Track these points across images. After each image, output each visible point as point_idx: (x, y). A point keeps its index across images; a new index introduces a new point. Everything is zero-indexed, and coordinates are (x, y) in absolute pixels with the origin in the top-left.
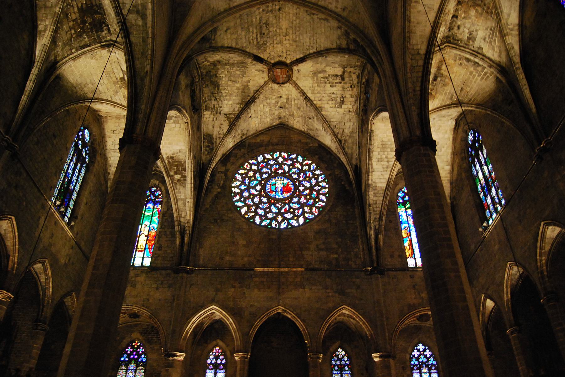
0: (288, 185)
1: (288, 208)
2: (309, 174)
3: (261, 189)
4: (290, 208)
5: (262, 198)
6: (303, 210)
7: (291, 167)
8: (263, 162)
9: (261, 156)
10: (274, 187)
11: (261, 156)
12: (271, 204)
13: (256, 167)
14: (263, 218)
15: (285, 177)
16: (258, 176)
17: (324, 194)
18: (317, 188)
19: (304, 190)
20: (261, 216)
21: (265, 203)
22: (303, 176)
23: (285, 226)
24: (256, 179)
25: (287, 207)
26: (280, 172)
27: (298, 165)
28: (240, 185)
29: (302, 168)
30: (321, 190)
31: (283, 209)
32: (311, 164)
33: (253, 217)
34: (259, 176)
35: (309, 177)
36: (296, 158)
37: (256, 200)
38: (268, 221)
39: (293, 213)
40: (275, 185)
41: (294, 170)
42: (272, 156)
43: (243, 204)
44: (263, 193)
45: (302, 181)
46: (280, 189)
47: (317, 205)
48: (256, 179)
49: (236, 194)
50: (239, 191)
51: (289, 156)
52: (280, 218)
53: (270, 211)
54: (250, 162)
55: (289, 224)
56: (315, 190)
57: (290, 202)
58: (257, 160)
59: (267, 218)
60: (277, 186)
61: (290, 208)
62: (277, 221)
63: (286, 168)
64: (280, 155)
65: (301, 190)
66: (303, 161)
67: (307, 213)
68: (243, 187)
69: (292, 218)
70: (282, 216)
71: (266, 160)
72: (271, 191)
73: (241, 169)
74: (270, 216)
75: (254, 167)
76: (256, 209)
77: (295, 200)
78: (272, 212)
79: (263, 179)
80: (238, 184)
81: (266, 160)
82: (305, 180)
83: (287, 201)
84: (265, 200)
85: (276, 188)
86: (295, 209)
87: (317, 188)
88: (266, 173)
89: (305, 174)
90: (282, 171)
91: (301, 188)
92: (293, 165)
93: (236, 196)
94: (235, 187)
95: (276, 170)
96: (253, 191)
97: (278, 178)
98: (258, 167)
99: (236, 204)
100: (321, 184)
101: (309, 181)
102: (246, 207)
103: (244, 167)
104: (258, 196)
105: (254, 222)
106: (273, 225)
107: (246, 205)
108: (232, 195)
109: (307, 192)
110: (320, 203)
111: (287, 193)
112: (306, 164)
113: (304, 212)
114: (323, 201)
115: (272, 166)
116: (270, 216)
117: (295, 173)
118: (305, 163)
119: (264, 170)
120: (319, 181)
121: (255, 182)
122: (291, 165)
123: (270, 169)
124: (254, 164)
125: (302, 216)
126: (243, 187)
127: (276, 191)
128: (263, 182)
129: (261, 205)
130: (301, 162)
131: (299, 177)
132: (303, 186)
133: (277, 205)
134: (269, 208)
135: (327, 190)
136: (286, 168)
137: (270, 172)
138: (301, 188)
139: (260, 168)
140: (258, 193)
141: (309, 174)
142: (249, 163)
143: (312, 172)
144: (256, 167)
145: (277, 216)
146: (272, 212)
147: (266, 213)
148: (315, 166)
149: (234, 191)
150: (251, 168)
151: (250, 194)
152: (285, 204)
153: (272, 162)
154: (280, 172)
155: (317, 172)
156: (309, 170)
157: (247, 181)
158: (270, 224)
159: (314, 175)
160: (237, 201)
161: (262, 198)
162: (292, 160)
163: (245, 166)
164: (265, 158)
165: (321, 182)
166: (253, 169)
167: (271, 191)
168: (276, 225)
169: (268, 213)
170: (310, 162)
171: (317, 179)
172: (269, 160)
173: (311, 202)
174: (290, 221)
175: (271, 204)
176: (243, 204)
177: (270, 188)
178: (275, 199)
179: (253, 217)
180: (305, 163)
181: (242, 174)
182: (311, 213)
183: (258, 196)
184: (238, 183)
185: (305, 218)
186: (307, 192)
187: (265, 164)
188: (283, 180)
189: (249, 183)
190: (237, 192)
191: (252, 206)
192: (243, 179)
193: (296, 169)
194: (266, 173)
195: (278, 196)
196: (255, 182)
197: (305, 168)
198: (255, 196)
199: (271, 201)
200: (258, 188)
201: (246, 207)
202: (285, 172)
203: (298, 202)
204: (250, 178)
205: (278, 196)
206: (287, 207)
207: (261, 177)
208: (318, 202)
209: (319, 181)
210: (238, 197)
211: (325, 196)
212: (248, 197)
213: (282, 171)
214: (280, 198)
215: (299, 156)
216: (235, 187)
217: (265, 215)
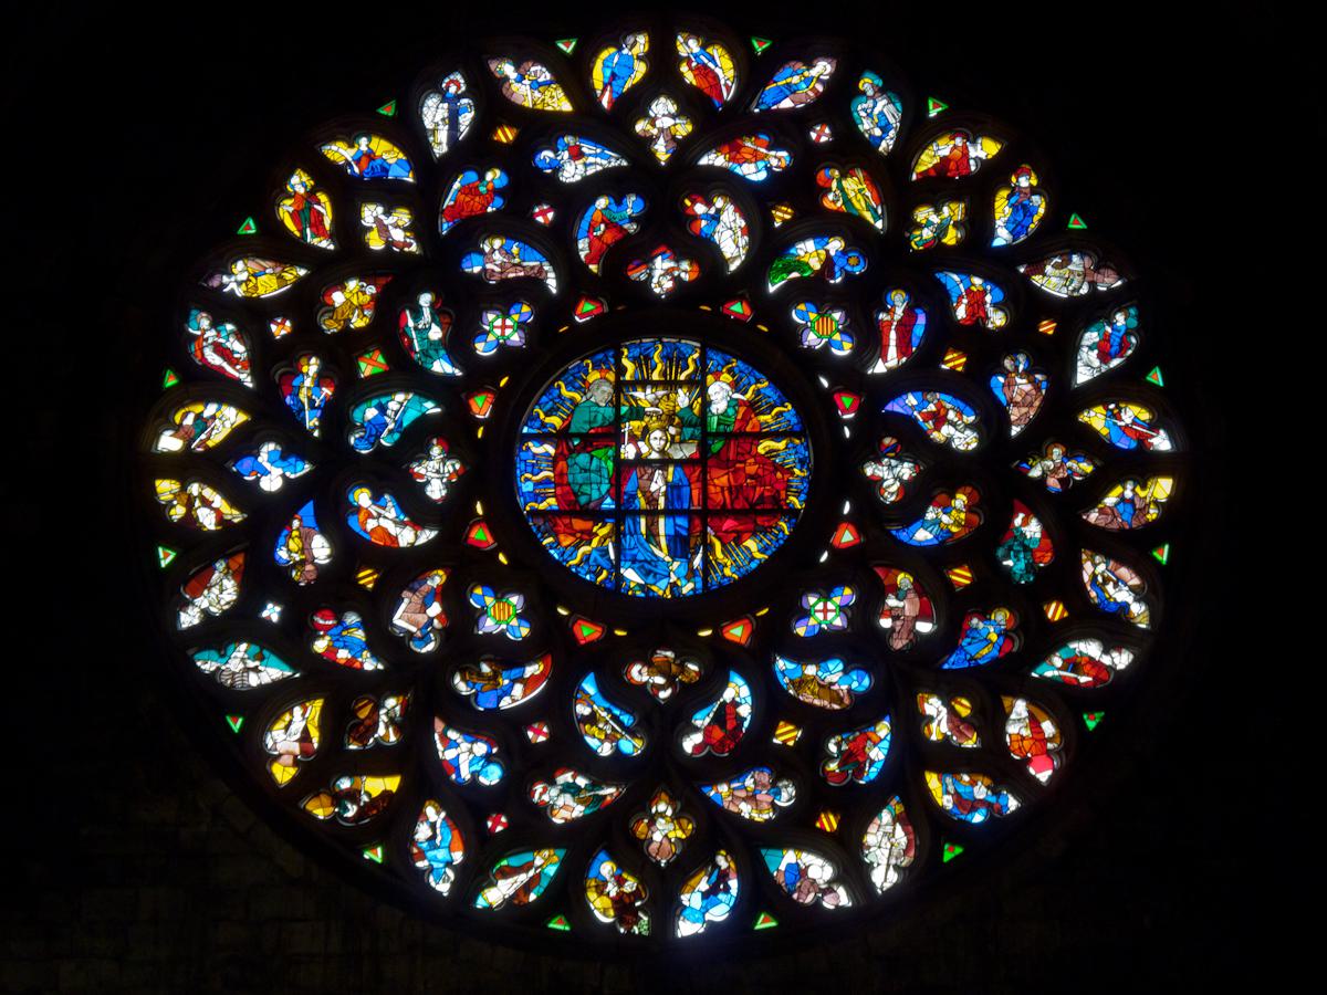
0: (741, 437)
1: (745, 711)
2: (976, 302)
3: (461, 491)
4: (773, 702)
5: (481, 597)
6: (910, 725)
7: (782, 215)
8: (473, 152)
9: (456, 83)
10: (603, 460)
11: (456, 83)
12: (568, 664)
13: (403, 216)
14: (498, 825)
15: (724, 340)
16: (425, 327)
17: (1126, 546)
18: (1052, 467)
19: (913, 502)
20: (467, 805)
21: (508, 655)
22: (905, 327)
23: (719, 913)
24: (407, 373)
25: (738, 691)
26: (663, 274)
27: (853, 192)
28: (242, 443)
29: (902, 221)
30: (1091, 490)
31: (702, 719)
32: (994, 175)
33: (393, 819)
34: (436, 333)
35: (973, 337)
36: (836, 102)
37: (414, 616)
38: (547, 863)
39: (800, 765)
40: (610, 435)
41: (809, 252)
42: (573, 76)
43: (273, 672)
44: (480, 534)
45: (897, 383)
46: (658, 485)
47: (1053, 668)
48: (407, 373)
49: (200, 551)
50: (235, 515)
51: (755, 74)
52: (664, 831)
53: (568, 751)
54: (339, 152)
55: (761, 891)
56: (1035, 498)
57: (776, 638)
58: (410, 135)
59: (533, 829)
60: (629, 452)
61: (773, 702)
62: (632, 855)
63: (730, 237)
64: (663, 65)
65: (891, 492)
66: (916, 133)
67: (949, 759)
68: (272, 474)
69: (793, 829)
70: (693, 805)
71: (505, 135)
72: (576, 510)
73: (249, 249)
74: (563, 802)
75: (387, 227)
76: (414, 728)
77: (825, 613)
78: (585, 761)
79: (479, 374)
80: (218, 435)
81: (505, 135)
82: (920, 373)
83: (737, 632)
84: (502, 616)
85: (623, 468)
86: (818, 724)
87: (1052, 467)
88: (507, 294)
89: (933, 299)
90: (686, 271)
91: (892, 475)
92: (799, 186)
93: (203, 585)
94: (186, 466)
95: (626, 251)
96: (380, 518)
97: (643, 361)
98: (422, 227)
99: (207, 664)
100: (1096, 418)
101: (974, 390)
102: (316, 707)
103: (271, 226)
104: (437, 579)
105: (403, 871)
106: (601, 908)
107: (318, 678)
108: (166, 557)
109: (947, 518)
110: (1092, 649)
111: (734, 540)
112: (940, 187)
113: (914, 755)
114: (1112, 629)
115: (574, 200)
116: (563, 802)
117: (814, 289)
118: (927, 160)
119: (495, 258)
120: (1083, 376)
121: (403, 407)
122: (778, 187)
123: (557, 243)
124: (388, 193)
125: (896, 805)
126: (272, 474)
127: (623, 514)
128: (481, 406)
129: (470, 672)
130: (886, 145)
131: (869, 340)
132: (912, 441)
133: (638, 673)
134: (556, 704)
135: (1162, 488)
136: (730, 237)
137: (552, 283)
138: (892, 475)
139: (445, 227)
140: (427, 535)
141: (976, 302)
142: (330, 178)
143: (1008, 269)
144: (403, 216)
145: (636, 805)
146: (585, 761)
147: (525, 766)
148: (1040, 204)
149: (178, 512)
150: (349, 229)
151: (352, 549)
152: (722, 661)
153: (577, 164)
154: (663, 274)
155: (1057, 280)
156: (975, 252)
157: (309, 385)
158: (568, 892)
159: (1025, 303)
160: (218, 632)
161: (481, 597)
162: (787, 129)
163: (285, 211)
164: (492, 102)
165: (1108, 390)
166: (376, 243)
167: (576, 510)
168: (623, 906)
169: (543, 765)
170: (986, 149)
171: (1055, 359)
172: (541, 127)
173: (989, 634)
174: (769, 856)
175: (568, 664)
176: (273, 672)
177: (560, 480)
178: (607, 601)
179: (393, 819)
180: (927, 160)
181: (250, 315)
182: (998, 764)
183: (437, 579)
184: (230, 418)
185: (926, 822)
186: (947, 518)
187: (494, 176)
188: (698, 384)
189: (337, 416)
190: (208, 520)
191: (376, 688)
192: (273, 362)
193: (835, 245)
194: (507, 294)
195: (649, 568)
196: (403, 407)
197: (937, 223)
198: (401, 569)
199: (564, 627)
200: (436, 474)
201: (316, 707)
202: (713, 276)
203: (857, 644)
204: (340, 352)
205: (649, 568)
206: (738, 691)
207: (458, 345)
208: (1056, 637)
209: (1083, 376)
210: (221, 593)
211: (1142, 564)
212: (334, 590)
213: (686, 271)
214: (660, 589)
215: (867, 83)
216: (186, 466)
217: (513, 795)
